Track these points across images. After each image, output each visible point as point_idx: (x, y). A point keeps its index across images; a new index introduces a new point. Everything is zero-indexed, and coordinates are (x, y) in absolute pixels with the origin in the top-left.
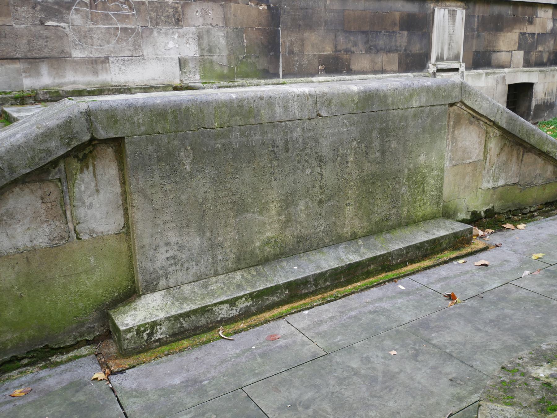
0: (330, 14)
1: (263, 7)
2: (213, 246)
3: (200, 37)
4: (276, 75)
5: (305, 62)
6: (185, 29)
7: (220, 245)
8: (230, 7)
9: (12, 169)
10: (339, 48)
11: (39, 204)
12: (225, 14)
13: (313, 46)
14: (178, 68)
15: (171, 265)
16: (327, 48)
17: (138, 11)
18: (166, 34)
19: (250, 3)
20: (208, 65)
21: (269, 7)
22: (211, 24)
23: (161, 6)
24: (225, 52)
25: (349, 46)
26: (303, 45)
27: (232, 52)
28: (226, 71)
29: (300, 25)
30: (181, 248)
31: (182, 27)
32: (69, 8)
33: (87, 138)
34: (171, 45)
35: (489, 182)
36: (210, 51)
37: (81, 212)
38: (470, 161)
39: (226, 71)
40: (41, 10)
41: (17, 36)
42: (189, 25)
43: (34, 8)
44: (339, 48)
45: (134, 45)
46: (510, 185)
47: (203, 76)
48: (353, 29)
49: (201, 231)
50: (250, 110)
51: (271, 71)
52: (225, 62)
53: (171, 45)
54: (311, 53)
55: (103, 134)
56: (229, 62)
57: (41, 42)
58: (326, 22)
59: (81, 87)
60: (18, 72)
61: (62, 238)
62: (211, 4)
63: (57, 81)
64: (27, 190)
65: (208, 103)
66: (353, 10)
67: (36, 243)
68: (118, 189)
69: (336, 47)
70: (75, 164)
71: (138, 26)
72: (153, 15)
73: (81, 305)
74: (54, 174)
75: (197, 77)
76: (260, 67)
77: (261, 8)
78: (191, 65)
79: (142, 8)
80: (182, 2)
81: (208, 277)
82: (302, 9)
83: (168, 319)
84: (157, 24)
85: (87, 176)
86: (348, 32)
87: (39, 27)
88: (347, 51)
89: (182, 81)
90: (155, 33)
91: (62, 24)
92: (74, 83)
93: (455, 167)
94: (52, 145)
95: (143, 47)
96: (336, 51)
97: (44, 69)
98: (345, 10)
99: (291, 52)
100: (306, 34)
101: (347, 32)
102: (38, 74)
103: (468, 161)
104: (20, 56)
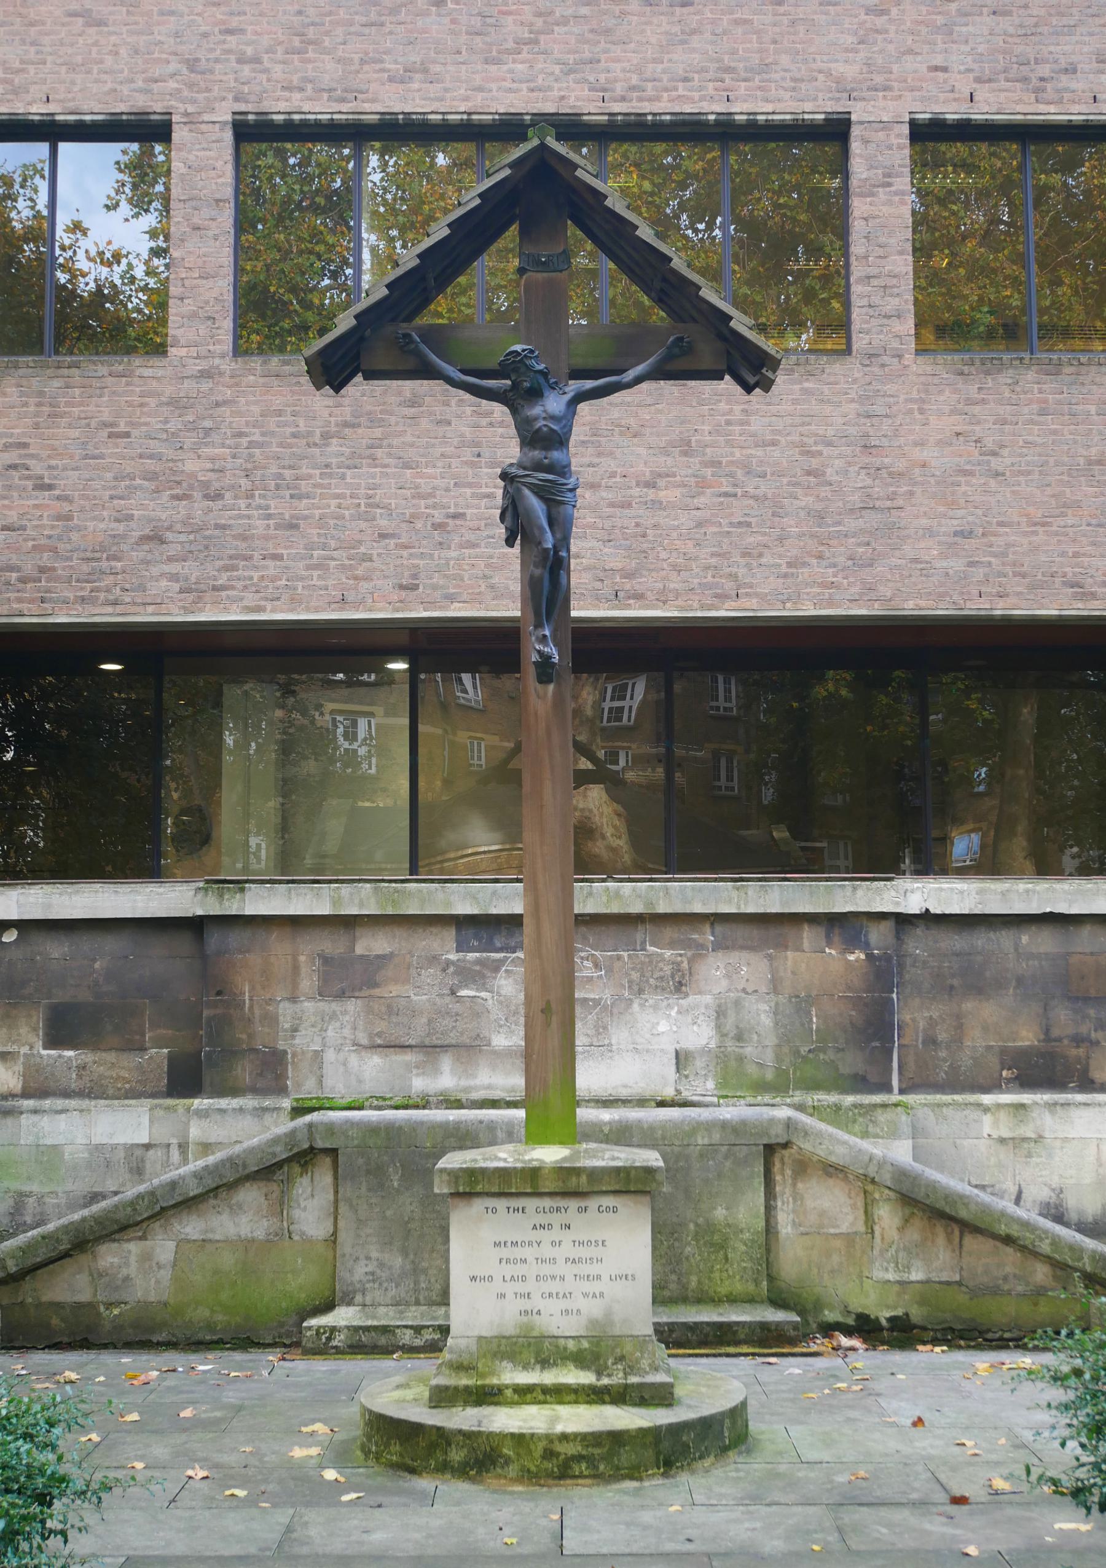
0: (1031, 963)
1: (857, 956)
2: (416, 1271)
3: (720, 1013)
4: (887, 1088)
5: (965, 1060)
6: (691, 999)
7: (425, 1271)
8: (786, 958)
9: (245, 1166)
10: (1055, 1032)
11: (263, 1199)
12: (774, 971)
13: (985, 1029)
14: (673, 1068)
15: (369, 1281)
16: (1024, 1033)
17: (610, 970)
18: (655, 1008)
19: (827, 950)
20: (733, 1064)
21: (870, 957)
22: (744, 990)
23: (651, 962)
24: (771, 1040)
25: (1084, 1029)
26: (960, 1027)
27: (784, 1039)
28: (770, 1076)
29: (952, 987)
30: (381, 1265)
31: (687, 995)
32: (497, 969)
33: (306, 1146)
34: (663, 1027)
35: (887, 1269)
36: (739, 1038)
37: (296, 1213)
38: (837, 1231)
39: (770, 1076)
40: (455, 973)
41: (414, 1013)
42: (700, 993)
43: (444, 970)
44: (1055, 1032)
45: (596, 1027)
46: (940, 1283)
47: (722, 1084)
48: (1093, 993)
49: (405, 1252)
50: (468, 1133)
51: (873, 1078)
52: (769, 1058)
53: (663, 1027)
54: (980, 1043)
55: (320, 1144)
56: (778, 1058)
57: (447, 1022)
58: (1020, 981)
59: (497, 1094)
60: (408, 1067)
61: (277, 1235)
62: (745, 955)
63: (464, 1083)
64: (255, 1186)
65: (422, 1123)
66: (1092, 954)
67: (255, 1234)
68: (331, 1197)
69: (1047, 1032)
70: (297, 1169)
71: (607, 995)
72: (635, 976)
73: (284, 1305)
74: (279, 1176)
75: (710, 1085)
76: (845, 1070)
77: (852, 957)
78: (699, 1063)
79: (617, 965)
80: (689, 954)
81: (407, 1304)
82: (957, 955)
83: (348, 1327)
84: (641, 991)
85: (305, 1181)
86: (1079, 999)
87: (448, 999)
88: (1078, 1040)
89: (679, 1092)
90: (636, 1006)
91: (483, 994)
92: (489, 1087)
93: (805, 1237)
94: (278, 1149)
95: (612, 1030)
96: (1048, 1037)
97: (446, 1063)
98: (1068, 954)
99: (931, 1041)
100: (968, 1005)
101: (1077, 999)
102: (437, 1072)
103: (832, 1231)
104: (412, 1042)
